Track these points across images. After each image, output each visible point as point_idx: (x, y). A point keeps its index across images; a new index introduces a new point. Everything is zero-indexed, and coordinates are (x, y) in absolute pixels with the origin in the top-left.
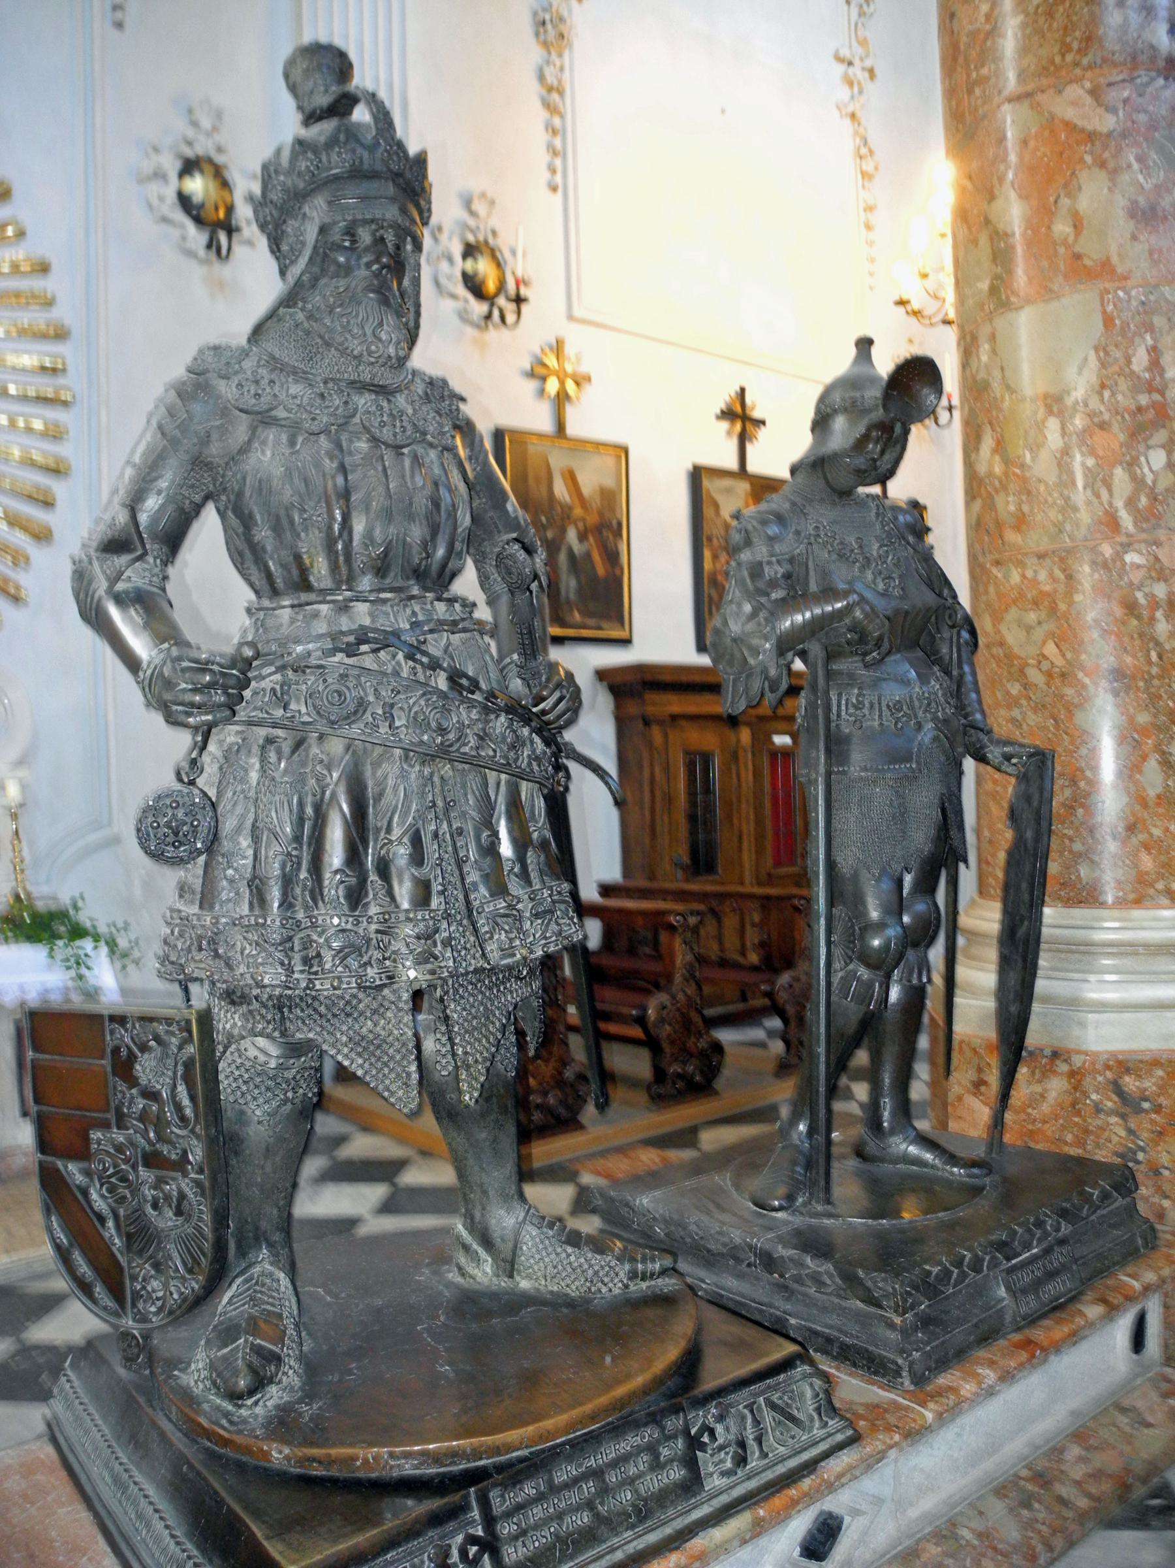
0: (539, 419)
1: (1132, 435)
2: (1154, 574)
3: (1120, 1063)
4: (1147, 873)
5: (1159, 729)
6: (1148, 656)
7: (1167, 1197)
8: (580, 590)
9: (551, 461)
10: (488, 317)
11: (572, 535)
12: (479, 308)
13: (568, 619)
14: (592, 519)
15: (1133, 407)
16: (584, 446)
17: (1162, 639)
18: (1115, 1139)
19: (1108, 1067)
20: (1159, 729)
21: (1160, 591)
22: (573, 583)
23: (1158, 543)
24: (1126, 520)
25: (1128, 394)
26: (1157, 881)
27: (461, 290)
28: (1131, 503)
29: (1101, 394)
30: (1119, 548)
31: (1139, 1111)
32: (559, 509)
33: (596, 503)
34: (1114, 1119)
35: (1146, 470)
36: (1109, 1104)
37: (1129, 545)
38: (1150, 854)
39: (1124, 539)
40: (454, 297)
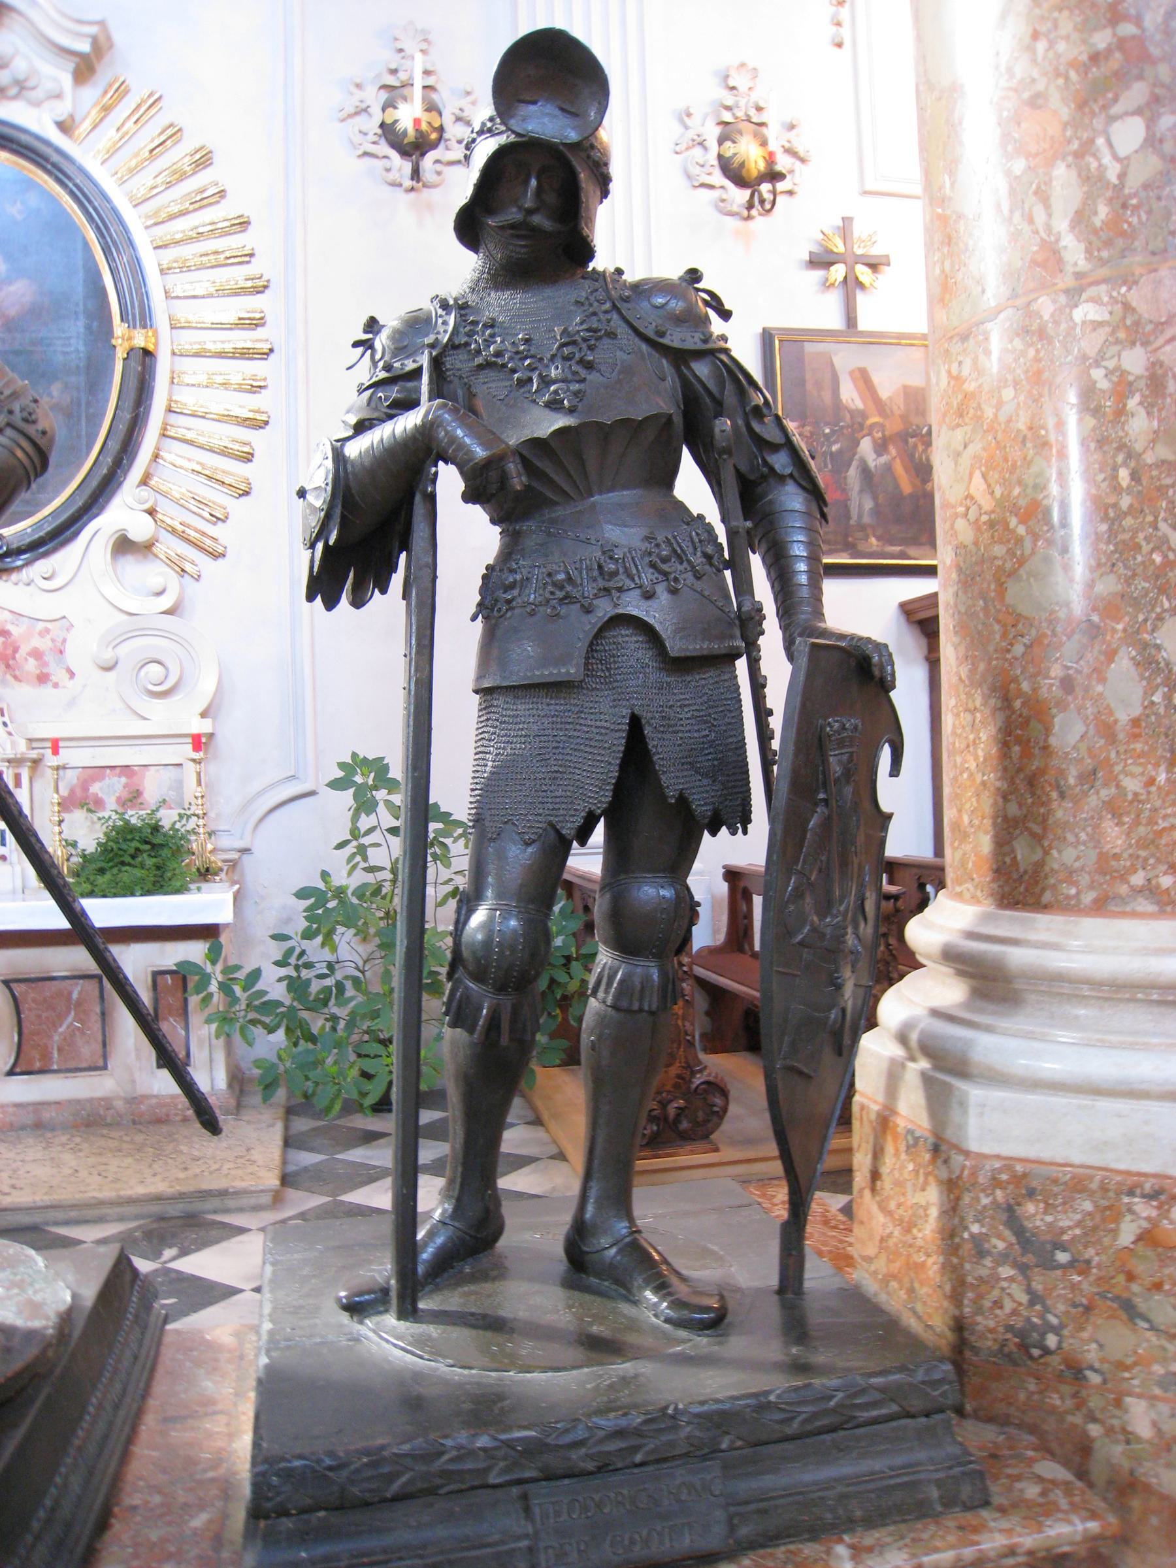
0: (825, 313)
1: (1082, 105)
3: (1019, 1180)
4: (1116, 857)
5: (1136, 603)
6: (1115, 477)
8: (877, 512)
9: (837, 361)
10: (750, 206)
11: (866, 446)
12: (740, 196)
13: (862, 546)
14: (894, 426)
16: (876, 340)
17: (1138, 447)
18: (1008, 1306)
19: (996, 1183)
20: (1136, 603)
21: (1135, 361)
22: (868, 504)
23: (1130, 281)
24: (1074, 252)
27: (718, 178)
28: (1080, 219)
30: (1063, 299)
31: (1049, 1264)
32: (848, 417)
33: (899, 407)
34: (1006, 1271)
35: (1107, 159)
36: (1001, 1245)
37: (1081, 290)
38: (1120, 824)
40: (711, 187)
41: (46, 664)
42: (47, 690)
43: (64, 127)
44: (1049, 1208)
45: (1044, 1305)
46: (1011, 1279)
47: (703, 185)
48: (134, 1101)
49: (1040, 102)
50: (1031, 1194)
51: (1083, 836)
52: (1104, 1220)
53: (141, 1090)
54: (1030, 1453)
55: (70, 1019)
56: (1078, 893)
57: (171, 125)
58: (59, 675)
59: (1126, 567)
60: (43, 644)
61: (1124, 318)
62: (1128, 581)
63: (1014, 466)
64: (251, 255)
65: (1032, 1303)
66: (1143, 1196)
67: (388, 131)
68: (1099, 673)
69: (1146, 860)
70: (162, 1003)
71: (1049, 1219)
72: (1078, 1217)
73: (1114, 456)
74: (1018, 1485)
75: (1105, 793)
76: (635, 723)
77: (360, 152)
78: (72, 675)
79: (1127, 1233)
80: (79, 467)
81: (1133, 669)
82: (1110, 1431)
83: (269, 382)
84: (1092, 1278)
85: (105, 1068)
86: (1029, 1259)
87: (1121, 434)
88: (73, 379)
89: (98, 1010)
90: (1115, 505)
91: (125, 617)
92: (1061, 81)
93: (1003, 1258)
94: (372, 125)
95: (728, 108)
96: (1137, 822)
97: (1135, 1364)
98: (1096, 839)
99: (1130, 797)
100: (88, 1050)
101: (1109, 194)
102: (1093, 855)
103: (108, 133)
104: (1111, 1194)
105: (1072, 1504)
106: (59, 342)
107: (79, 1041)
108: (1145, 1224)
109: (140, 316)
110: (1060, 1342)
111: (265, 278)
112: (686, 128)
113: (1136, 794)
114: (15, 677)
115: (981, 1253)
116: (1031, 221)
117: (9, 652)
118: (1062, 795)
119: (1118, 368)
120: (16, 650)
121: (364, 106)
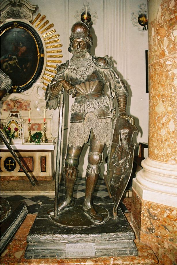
1: (169, 27)
2: (174, 67)
3: (150, 205)
6: (172, 91)
7: (159, 244)
10: (144, 29)
15: (169, 19)
25: (168, 16)
26: (172, 156)
28: (168, 47)
29: (162, 18)
30: (165, 60)
31: (154, 219)
34: (147, 219)
35: (172, 37)
37: (168, 59)
39: (166, 58)
41: (27, 107)
42: (27, 111)
43: (30, 22)
44: (154, 210)
45: (152, 225)
46: (148, 220)
47: (135, 26)
49: (163, 27)
50: (151, 207)
51: (164, 150)
52: (162, 213)
54: (148, 248)
56: (164, 159)
58: (28, 109)
59: (173, 106)
60: (26, 104)
61: (174, 64)
62: (173, 108)
63: (157, 87)
65: (151, 224)
66: (168, 210)
68: (168, 123)
69: (174, 155)
71: (154, 212)
72: (158, 212)
73: (171, 87)
74: (144, 253)
75: (168, 143)
76: (91, 130)
78: (31, 109)
79: (165, 215)
80: (33, 76)
81: (173, 123)
82: (162, 246)
84: (160, 222)
86: (151, 218)
87: (173, 83)
90: (172, 95)
92: (166, 23)
93: (147, 217)
95: (140, 12)
96: (173, 148)
97: (166, 236)
98: (166, 151)
99: (172, 144)
101: (172, 43)
102: (166, 153)
104: (163, 209)
105: (151, 257)
108: (168, 214)
109: (42, 51)
110: (155, 231)
112: (133, 16)
113: (173, 144)
114: (22, 109)
115: (144, 216)
116: (160, 47)
117: (21, 105)
118: (162, 143)
119: (173, 72)
120: (22, 105)
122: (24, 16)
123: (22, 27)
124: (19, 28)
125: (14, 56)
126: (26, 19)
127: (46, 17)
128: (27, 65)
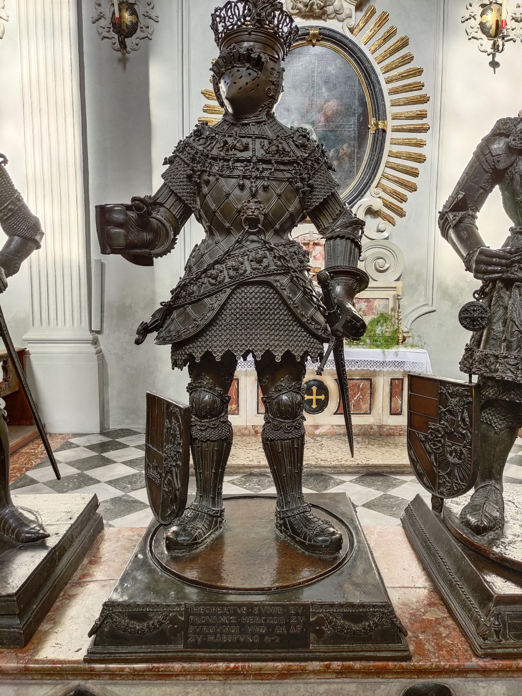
43: (351, 30)
48: (381, 427)
53: (384, 423)
55: (358, 395)
57: (392, 27)
64: (423, 86)
67: (483, 27)
70: (394, 390)
77: (470, 37)
83: (426, 143)
85: (370, 414)
88: (352, 142)
89: (369, 392)
91: (370, 240)
94: (475, 23)
100: (365, 407)
103: (367, 32)
106: (347, 127)
107: (361, 404)
111: (428, 96)
121: (473, 14)
122: (337, 12)
123: (328, 44)
124: (321, 45)
125: (307, 123)
126: (339, 20)
127: (389, 17)
128: (341, 151)
